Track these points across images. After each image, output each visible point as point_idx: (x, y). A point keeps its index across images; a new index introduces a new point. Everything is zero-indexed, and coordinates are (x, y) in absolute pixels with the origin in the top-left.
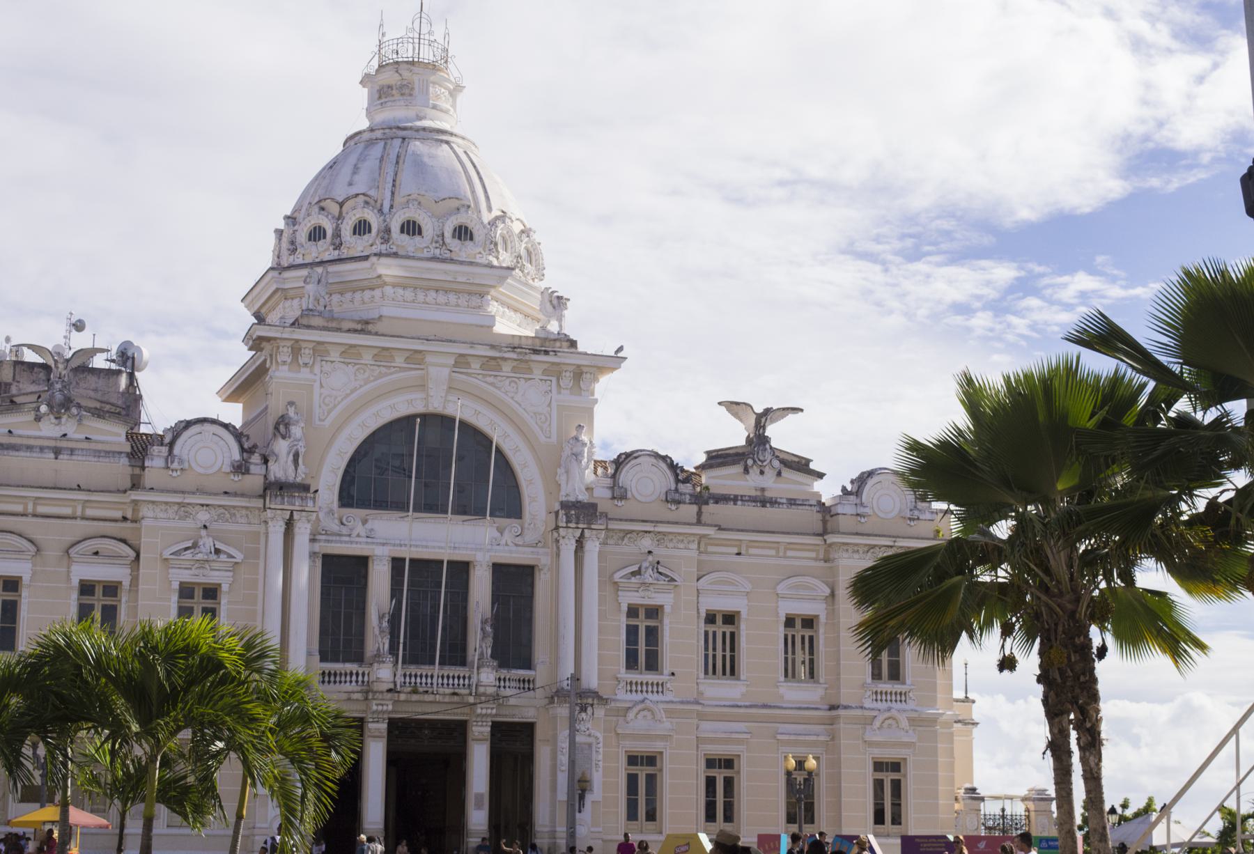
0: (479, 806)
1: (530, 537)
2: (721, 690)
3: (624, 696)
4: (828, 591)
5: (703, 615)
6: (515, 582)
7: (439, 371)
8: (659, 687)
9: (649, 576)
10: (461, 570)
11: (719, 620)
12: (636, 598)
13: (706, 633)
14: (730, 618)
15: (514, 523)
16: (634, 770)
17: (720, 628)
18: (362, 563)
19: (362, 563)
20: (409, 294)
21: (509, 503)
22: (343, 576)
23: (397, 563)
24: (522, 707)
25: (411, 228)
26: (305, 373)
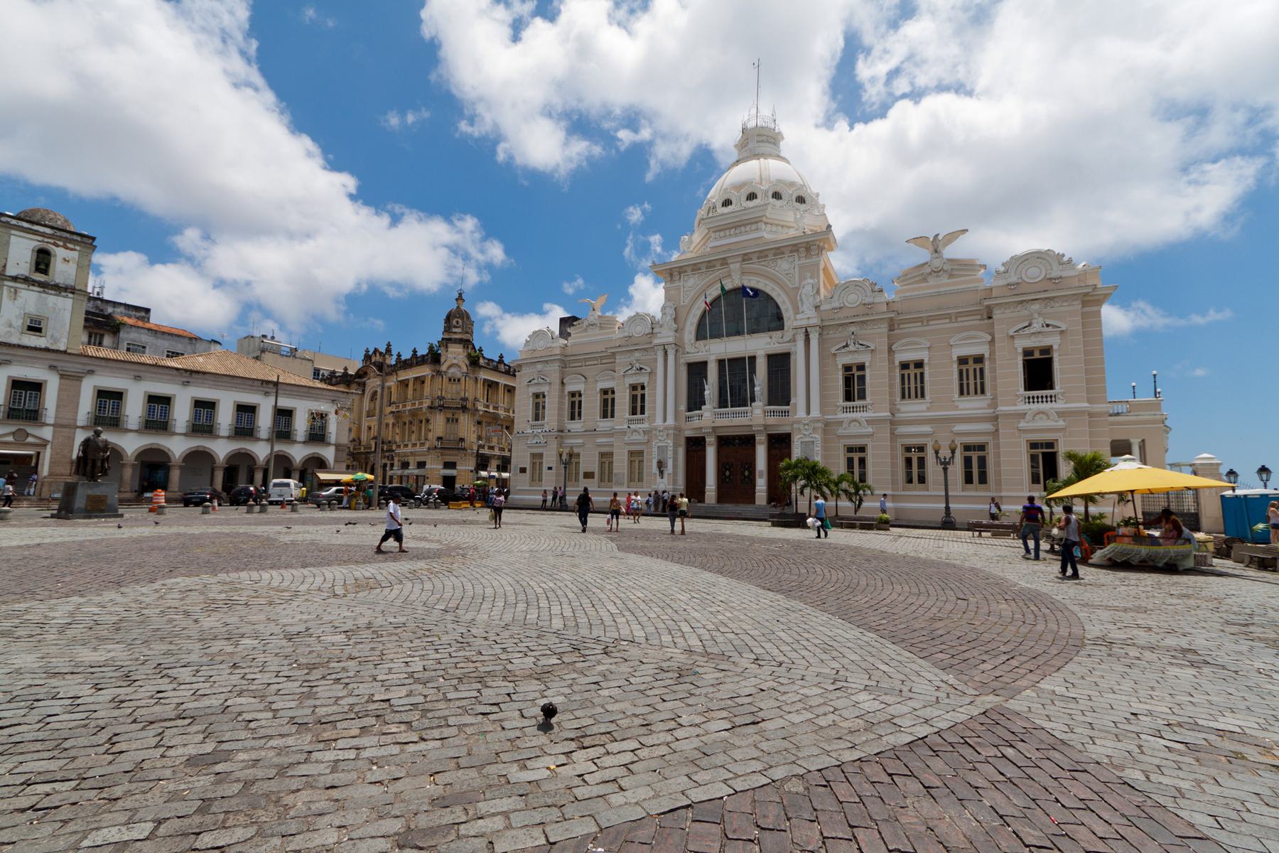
0: (761, 477)
1: (787, 338)
2: (912, 408)
3: (841, 416)
4: (989, 338)
5: (897, 363)
6: (780, 363)
7: (735, 267)
8: (864, 408)
9: (852, 348)
10: (753, 359)
11: (912, 366)
12: (849, 360)
13: (903, 376)
14: (919, 365)
15: (779, 333)
16: (851, 455)
17: (912, 371)
18: (705, 363)
19: (705, 363)
20: (722, 234)
21: (776, 321)
22: (697, 371)
23: (721, 362)
24: (779, 424)
25: (727, 203)
26: (677, 284)
